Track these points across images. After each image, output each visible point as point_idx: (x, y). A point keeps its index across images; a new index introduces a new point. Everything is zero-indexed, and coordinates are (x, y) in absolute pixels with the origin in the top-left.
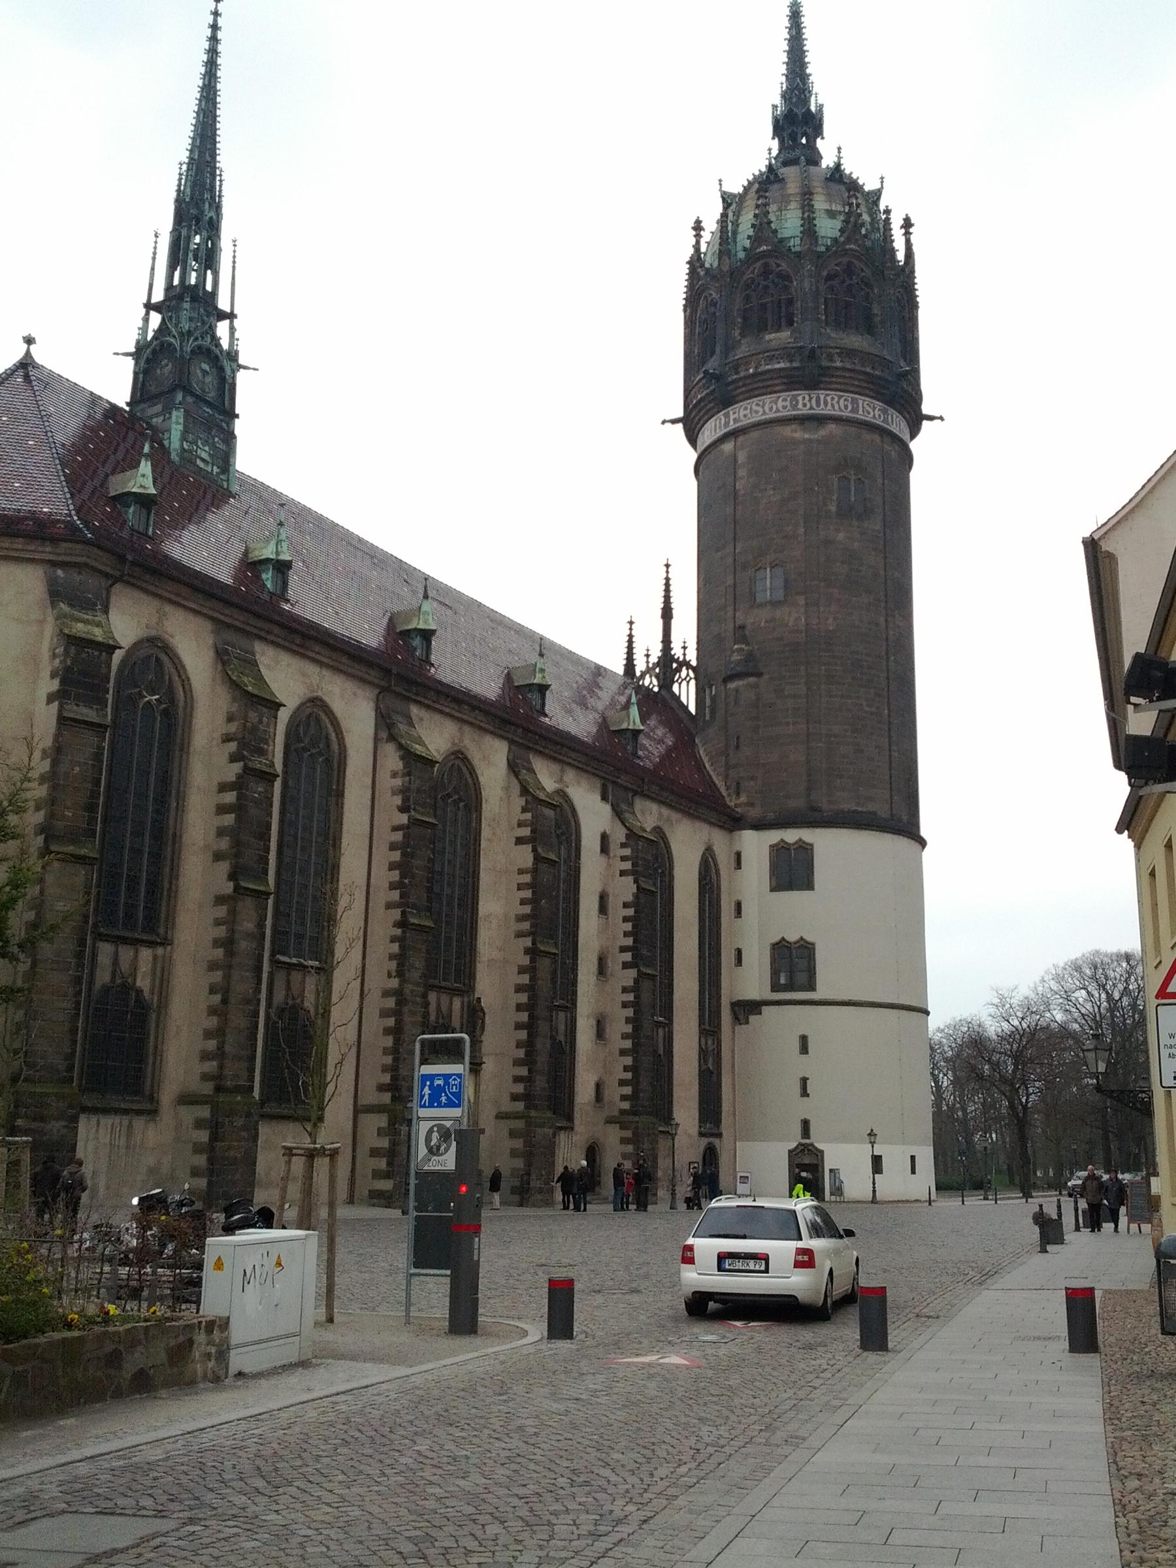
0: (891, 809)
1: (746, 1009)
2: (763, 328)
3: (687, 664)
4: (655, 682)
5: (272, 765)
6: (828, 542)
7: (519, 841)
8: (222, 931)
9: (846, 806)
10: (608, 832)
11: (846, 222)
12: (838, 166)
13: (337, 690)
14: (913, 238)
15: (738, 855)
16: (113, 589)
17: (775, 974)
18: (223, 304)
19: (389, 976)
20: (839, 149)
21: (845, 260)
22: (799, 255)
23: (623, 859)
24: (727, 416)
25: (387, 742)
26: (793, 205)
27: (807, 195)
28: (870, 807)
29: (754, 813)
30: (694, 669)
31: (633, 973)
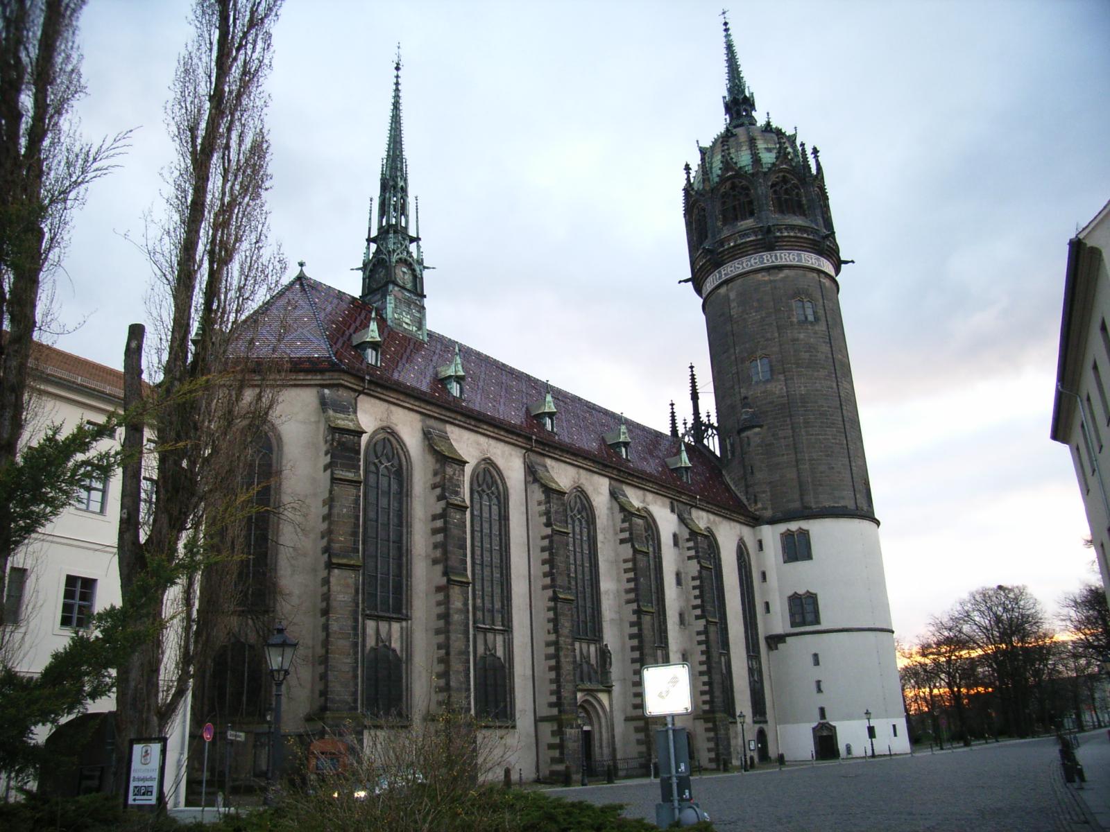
0: (856, 503)
1: (775, 641)
2: (736, 219)
3: (711, 426)
4: (692, 439)
5: (464, 501)
6: (795, 340)
7: (622, 541)
8: (441, 609)
9: (827, 504)
10: (677, 533)
11: (779, 152)
12: (768, 124)
13: (499, 452)
14: (819, 158)
15: (760, 542)
16: (358, 398)
17: (792, 615)
18: (412, 233)
19: (549, 632)
20: (768, 113)
21: (781, 174)
22: (752, 175)
23: (689, 549)
24: (720, 272)
25: (533, 483)
26: (744, 148)
27: (752, 142)
28: (842, 503)
29: (768, 513)
30: (716, 429)
31: (702, 622)
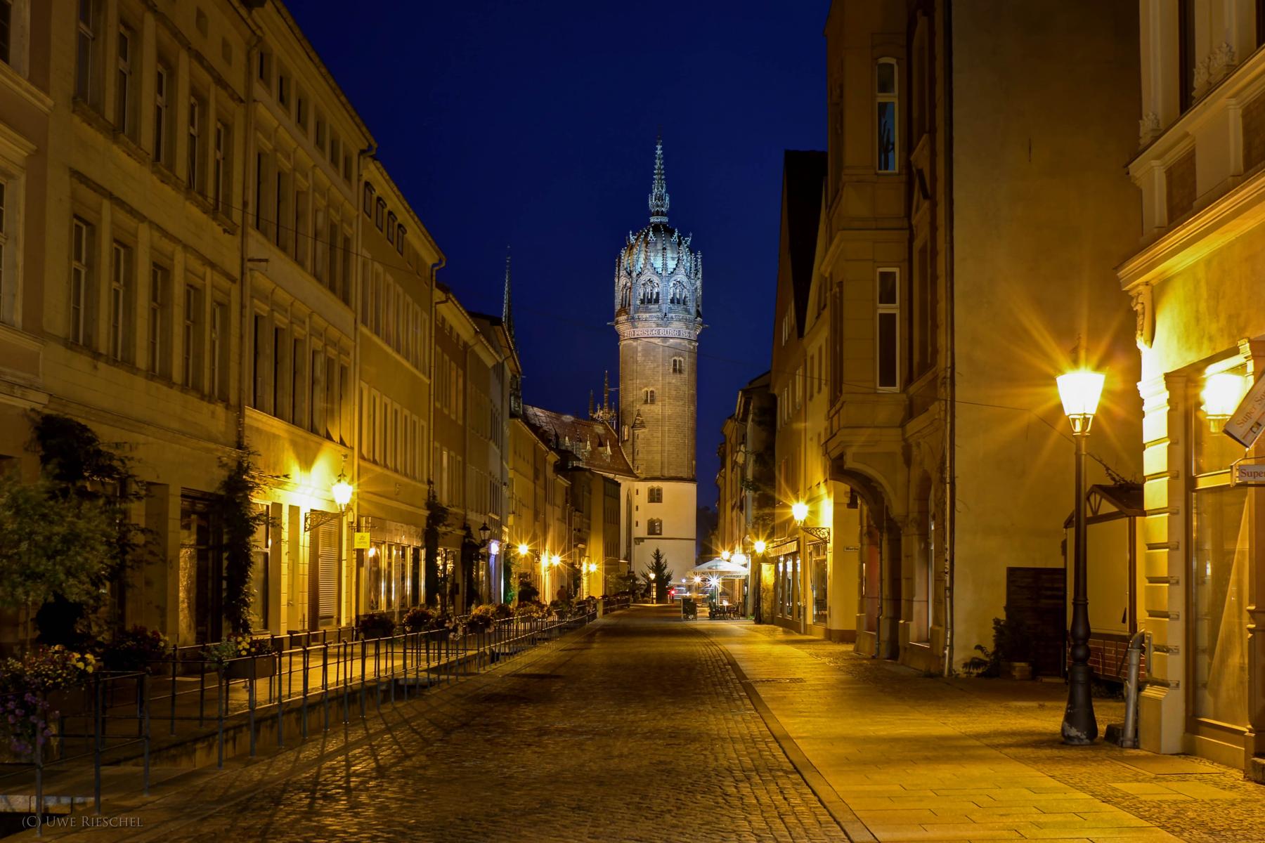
6: (669, 383)
17: (649, 529)
29: (643, 476)
